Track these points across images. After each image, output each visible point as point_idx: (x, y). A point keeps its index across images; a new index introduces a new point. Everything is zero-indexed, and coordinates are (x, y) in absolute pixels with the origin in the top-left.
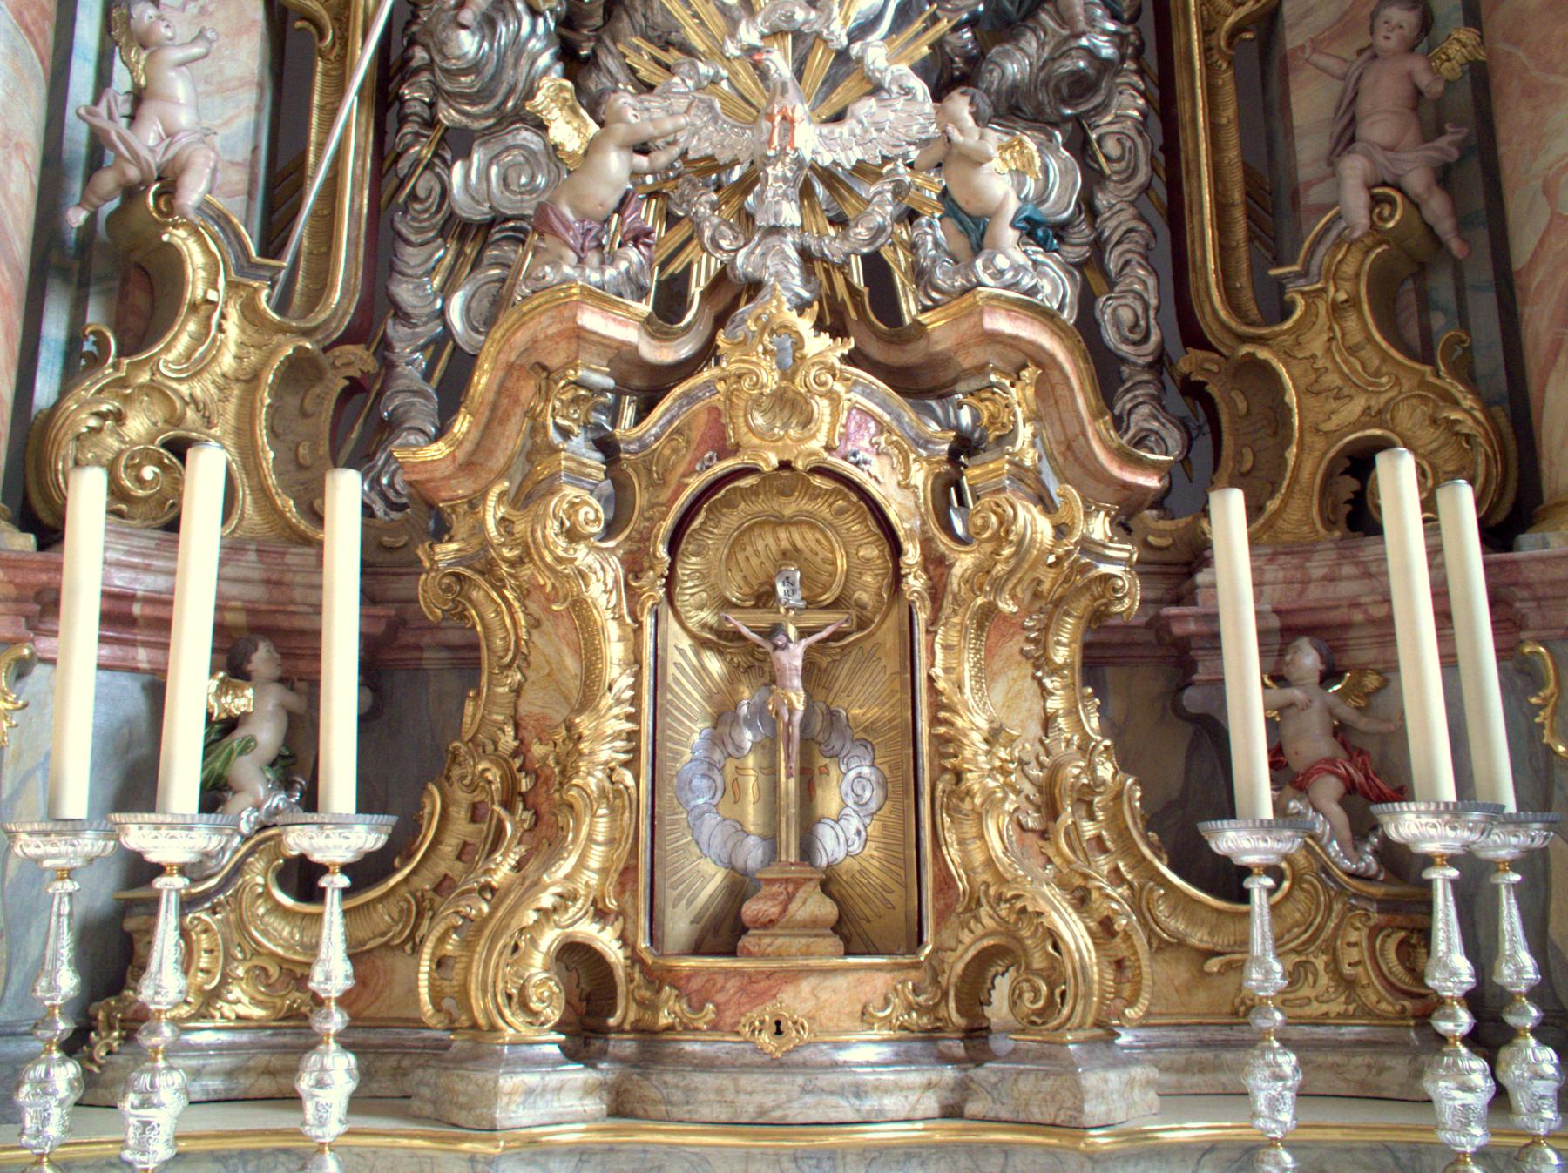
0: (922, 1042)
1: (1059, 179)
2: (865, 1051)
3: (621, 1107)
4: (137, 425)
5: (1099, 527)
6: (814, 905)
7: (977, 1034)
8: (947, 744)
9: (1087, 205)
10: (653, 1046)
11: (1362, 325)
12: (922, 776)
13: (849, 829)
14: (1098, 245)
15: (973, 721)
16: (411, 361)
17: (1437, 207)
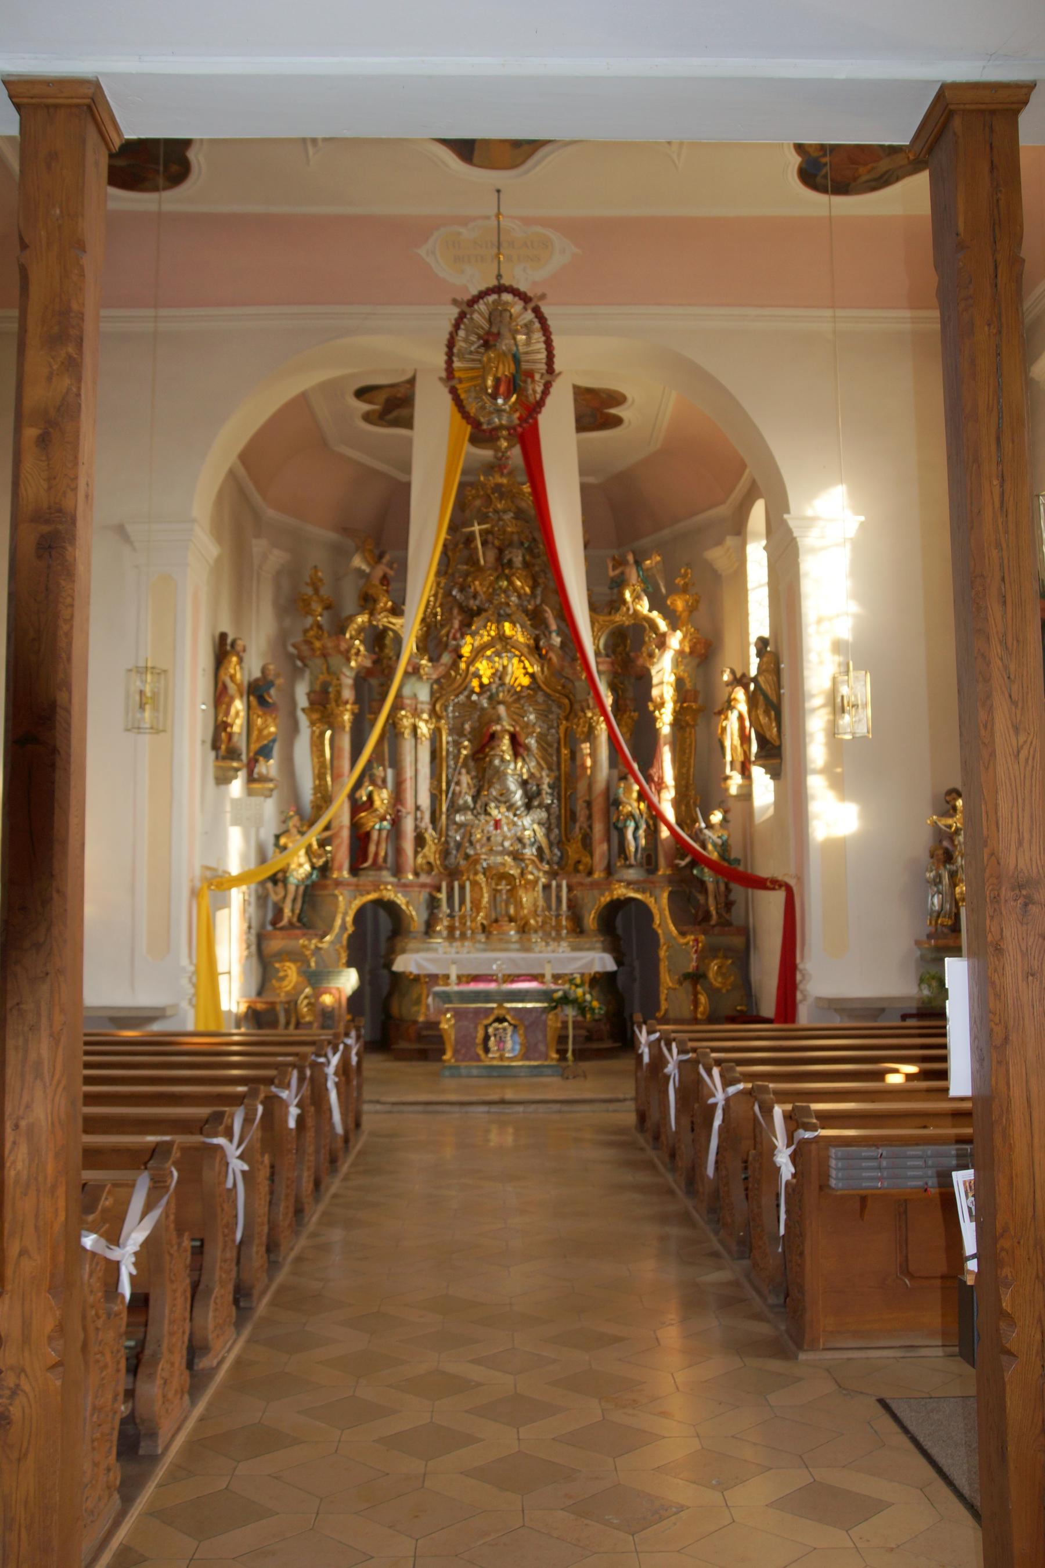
0: (518, 932)
1: (544, 815)
2: (512, 933)
3: (487, 938)
4: (424, 861)
5: (541, 874)
6: (506, 919)
7: (524, 932)
8: (521, 901)
9: (548, 818)
10: (490, 933)
11: (579, 844)
12: (519, 905)
13: (512, 911)
14: (550, 824)
15: (524, 900)
16: (452, 844)
17: (588, 830)
